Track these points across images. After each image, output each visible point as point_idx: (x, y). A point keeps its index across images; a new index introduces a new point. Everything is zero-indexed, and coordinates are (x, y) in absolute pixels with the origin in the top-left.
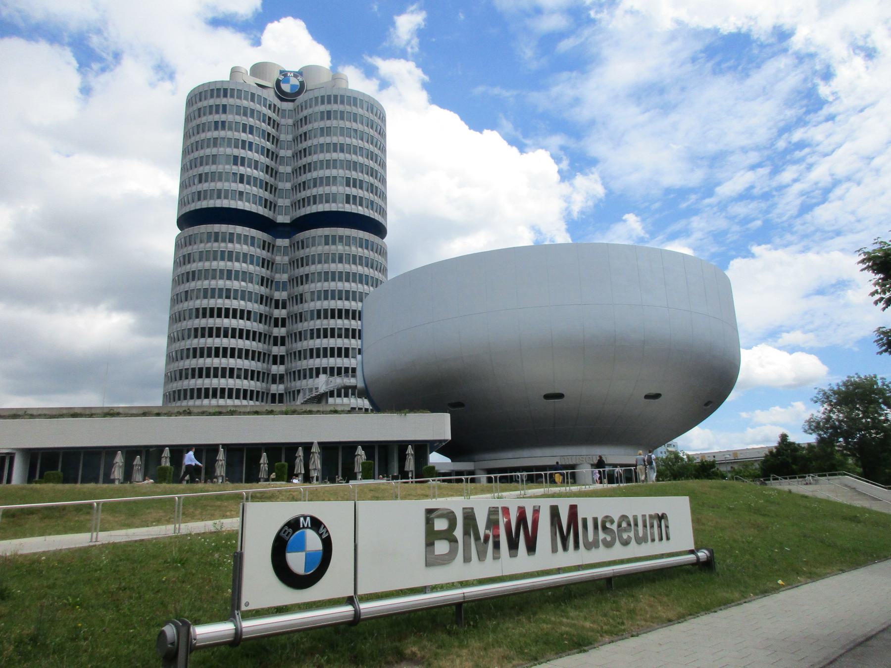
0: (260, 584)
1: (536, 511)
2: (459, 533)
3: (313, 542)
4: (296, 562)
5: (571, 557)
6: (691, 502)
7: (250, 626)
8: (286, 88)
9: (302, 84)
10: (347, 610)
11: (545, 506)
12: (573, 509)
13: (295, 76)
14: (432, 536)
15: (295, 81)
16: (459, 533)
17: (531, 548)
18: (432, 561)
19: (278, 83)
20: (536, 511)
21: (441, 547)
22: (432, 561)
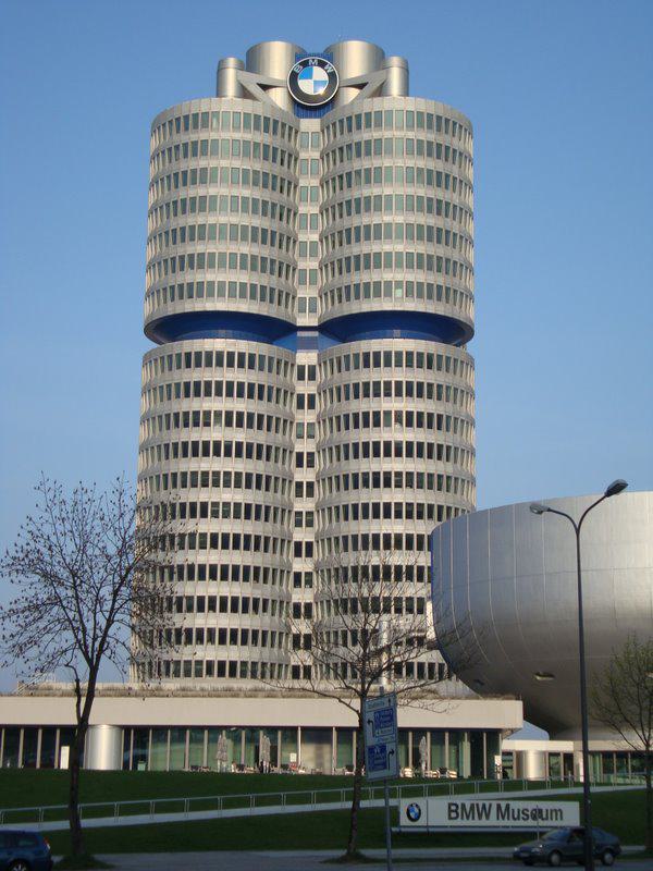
0: (404, 821)
1: (490, 805)
2: (460, 811)
3: (416, 810)
4: (412, 815)
5: (506, 822)
6: (580, 807)
7: (403, 830)
8: (306, 86)
9: (332, 76)
10: (425, 830)
11: (494, 804)
12: (508, 806)
13: (322, 64)
14: (450, 811)
15: (320, 74)
16: (460, 811)
17: (488, 817)
18: (450, 818)
19: (294, 77)
20: (490, 805)
21: (453, 815)
22: (450, 818)
